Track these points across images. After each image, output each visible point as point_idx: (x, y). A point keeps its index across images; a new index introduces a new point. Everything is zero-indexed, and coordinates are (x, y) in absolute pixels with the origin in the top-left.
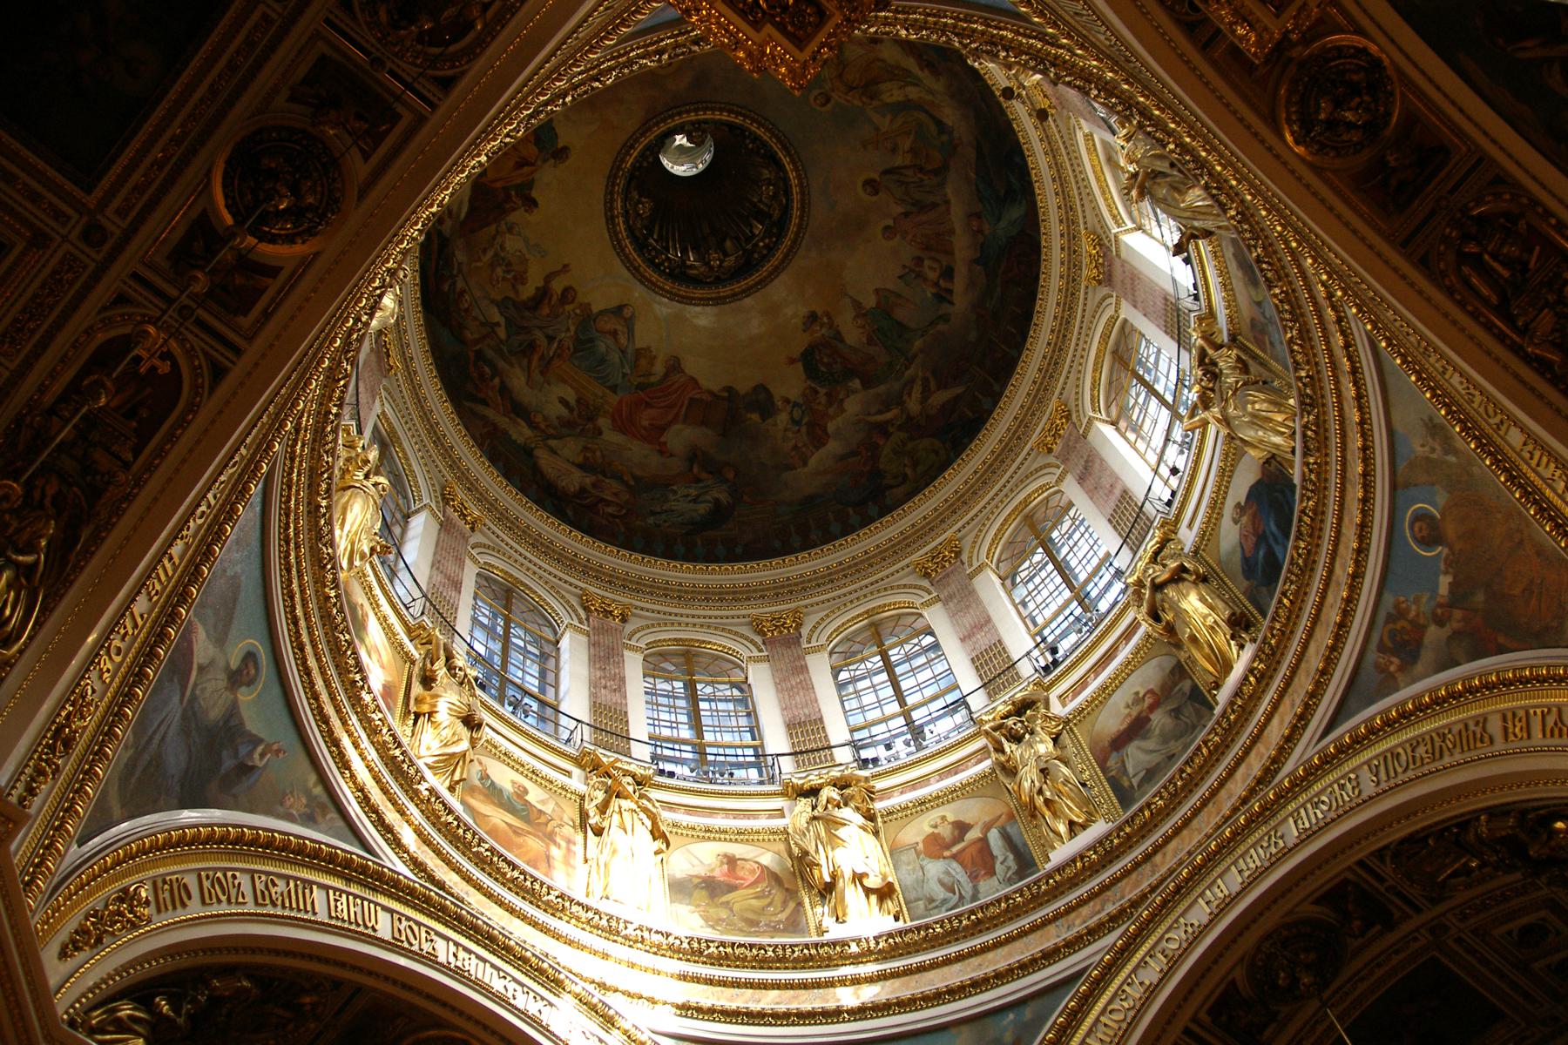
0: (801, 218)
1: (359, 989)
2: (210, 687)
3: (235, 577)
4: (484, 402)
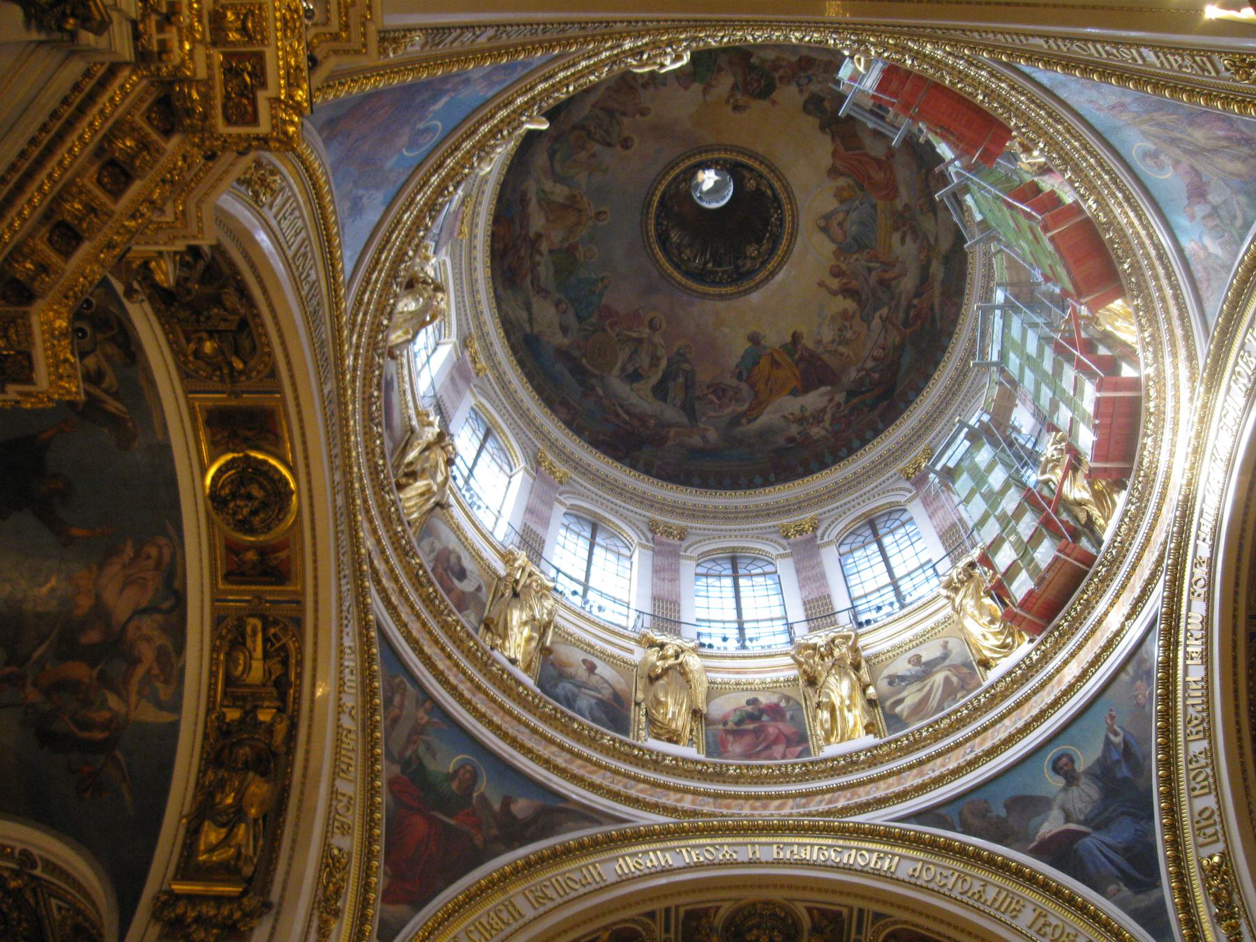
0: (683, 160)
2: (1079, 805)
3: (1006, 806)
4: (932, 309)
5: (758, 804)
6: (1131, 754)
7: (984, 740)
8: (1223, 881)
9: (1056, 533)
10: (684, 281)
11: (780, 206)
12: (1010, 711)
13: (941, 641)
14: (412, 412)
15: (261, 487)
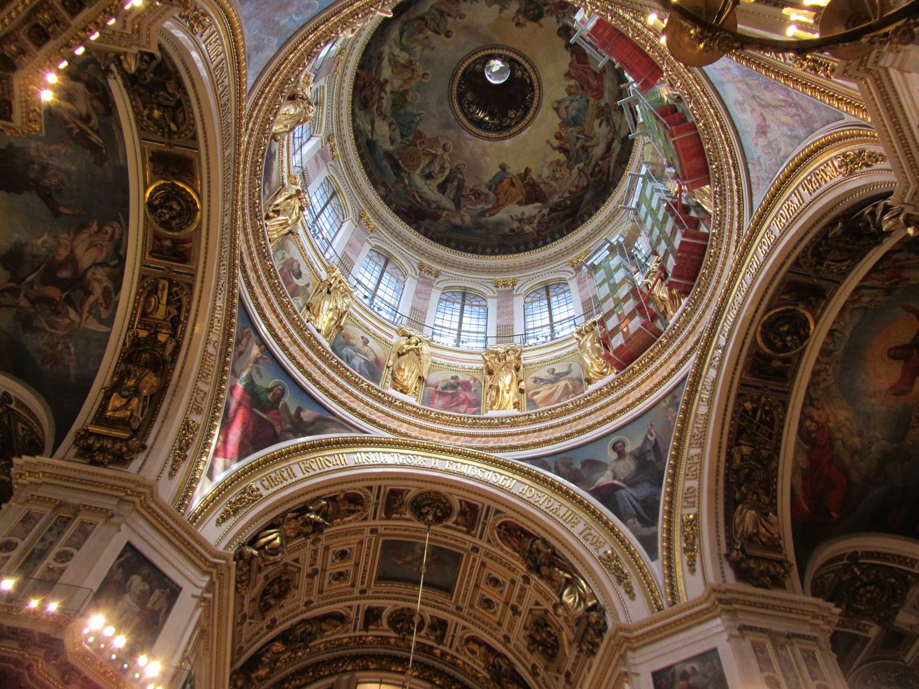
1: (742, 385)
2: (622, 471)
4: (609, 168)
5: (444, 436)
6: (657, 449)
7: (578, 424)
8: (692, 529)
9: (643, 314)
10: (468, 125)
11: (533, 90)
12: (597, 410)
13: (568, 363)
14: (285, 175)
15: (179, 204)
